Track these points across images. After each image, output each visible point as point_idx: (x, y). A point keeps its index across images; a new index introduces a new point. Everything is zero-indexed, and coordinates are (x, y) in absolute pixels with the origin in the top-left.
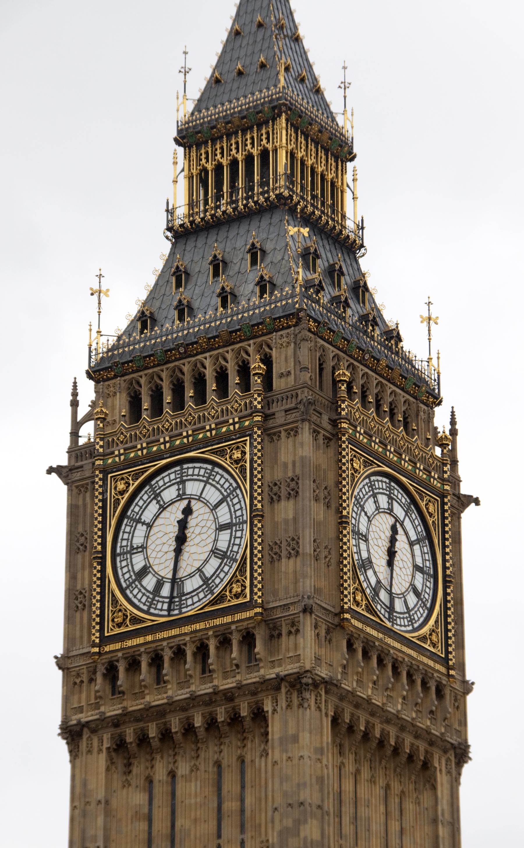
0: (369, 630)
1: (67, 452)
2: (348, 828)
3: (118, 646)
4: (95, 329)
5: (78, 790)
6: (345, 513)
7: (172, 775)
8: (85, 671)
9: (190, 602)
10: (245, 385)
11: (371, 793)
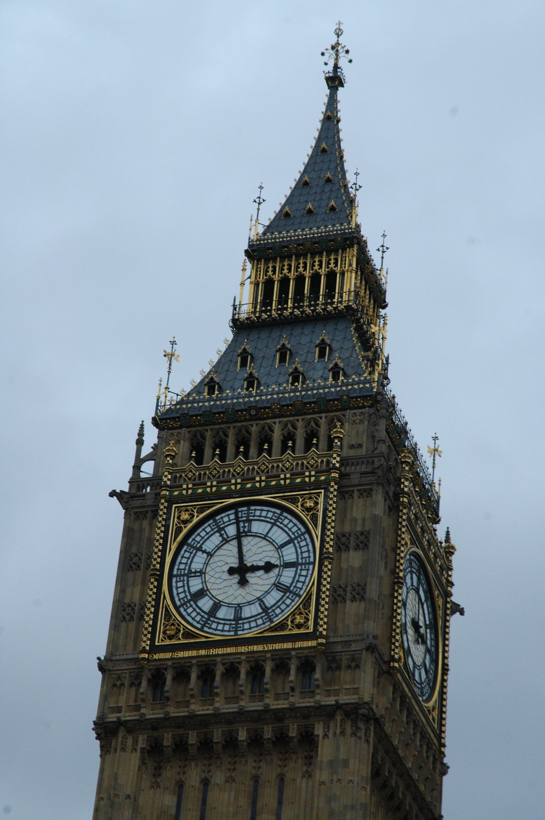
1: (129, 482)
3: (168, 655)
4: (164, 385)
5: (105, 784)
7: (205, 782)
8: (127, 675)
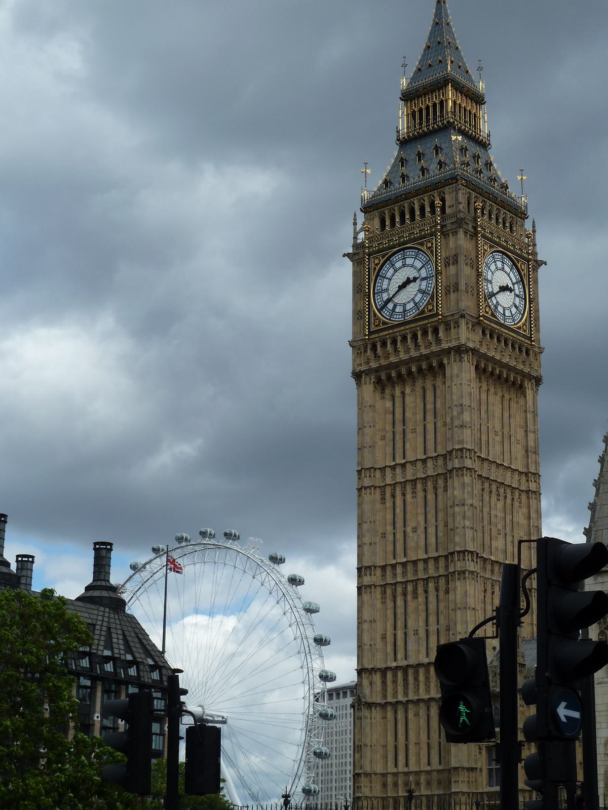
0: (492, 325)
2: (483, 415)
3: (377, 335)
6: (480, 270)
7: (403, 393)
9: (409, 314)
10: (433, 211)
11: (495, 399)
